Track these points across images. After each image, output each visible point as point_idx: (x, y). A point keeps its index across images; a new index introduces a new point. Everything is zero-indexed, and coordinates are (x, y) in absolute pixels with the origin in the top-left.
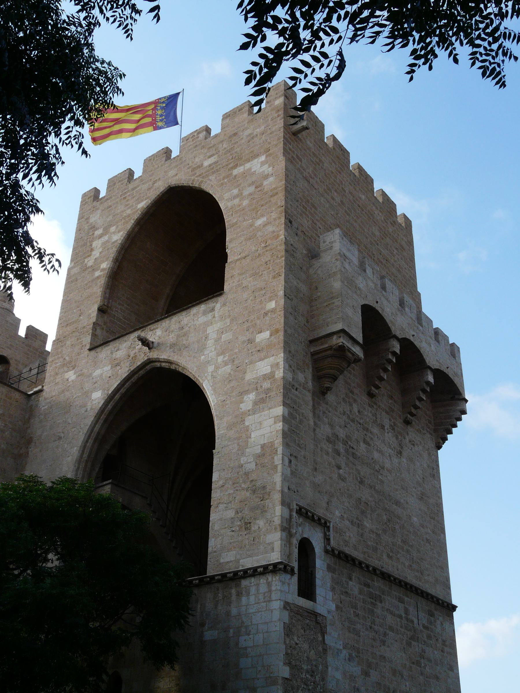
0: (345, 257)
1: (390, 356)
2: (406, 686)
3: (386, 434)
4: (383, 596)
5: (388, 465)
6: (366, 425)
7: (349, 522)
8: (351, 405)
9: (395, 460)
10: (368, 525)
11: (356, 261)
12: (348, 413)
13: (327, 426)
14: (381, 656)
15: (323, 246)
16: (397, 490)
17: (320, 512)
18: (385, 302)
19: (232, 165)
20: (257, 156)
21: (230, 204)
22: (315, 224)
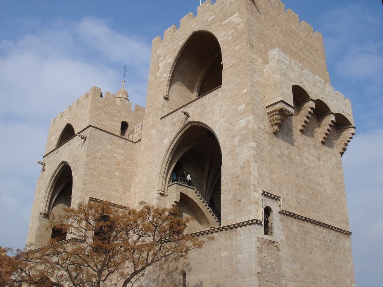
2: (323, 272)
5: (312, 165)
9: (317, 163)
10: (302, 197)
14: (310, 259)
15: (270, 57)
19: (222, 19)
20: (233, 13)
21: (222, 40)
22: (267, 45)
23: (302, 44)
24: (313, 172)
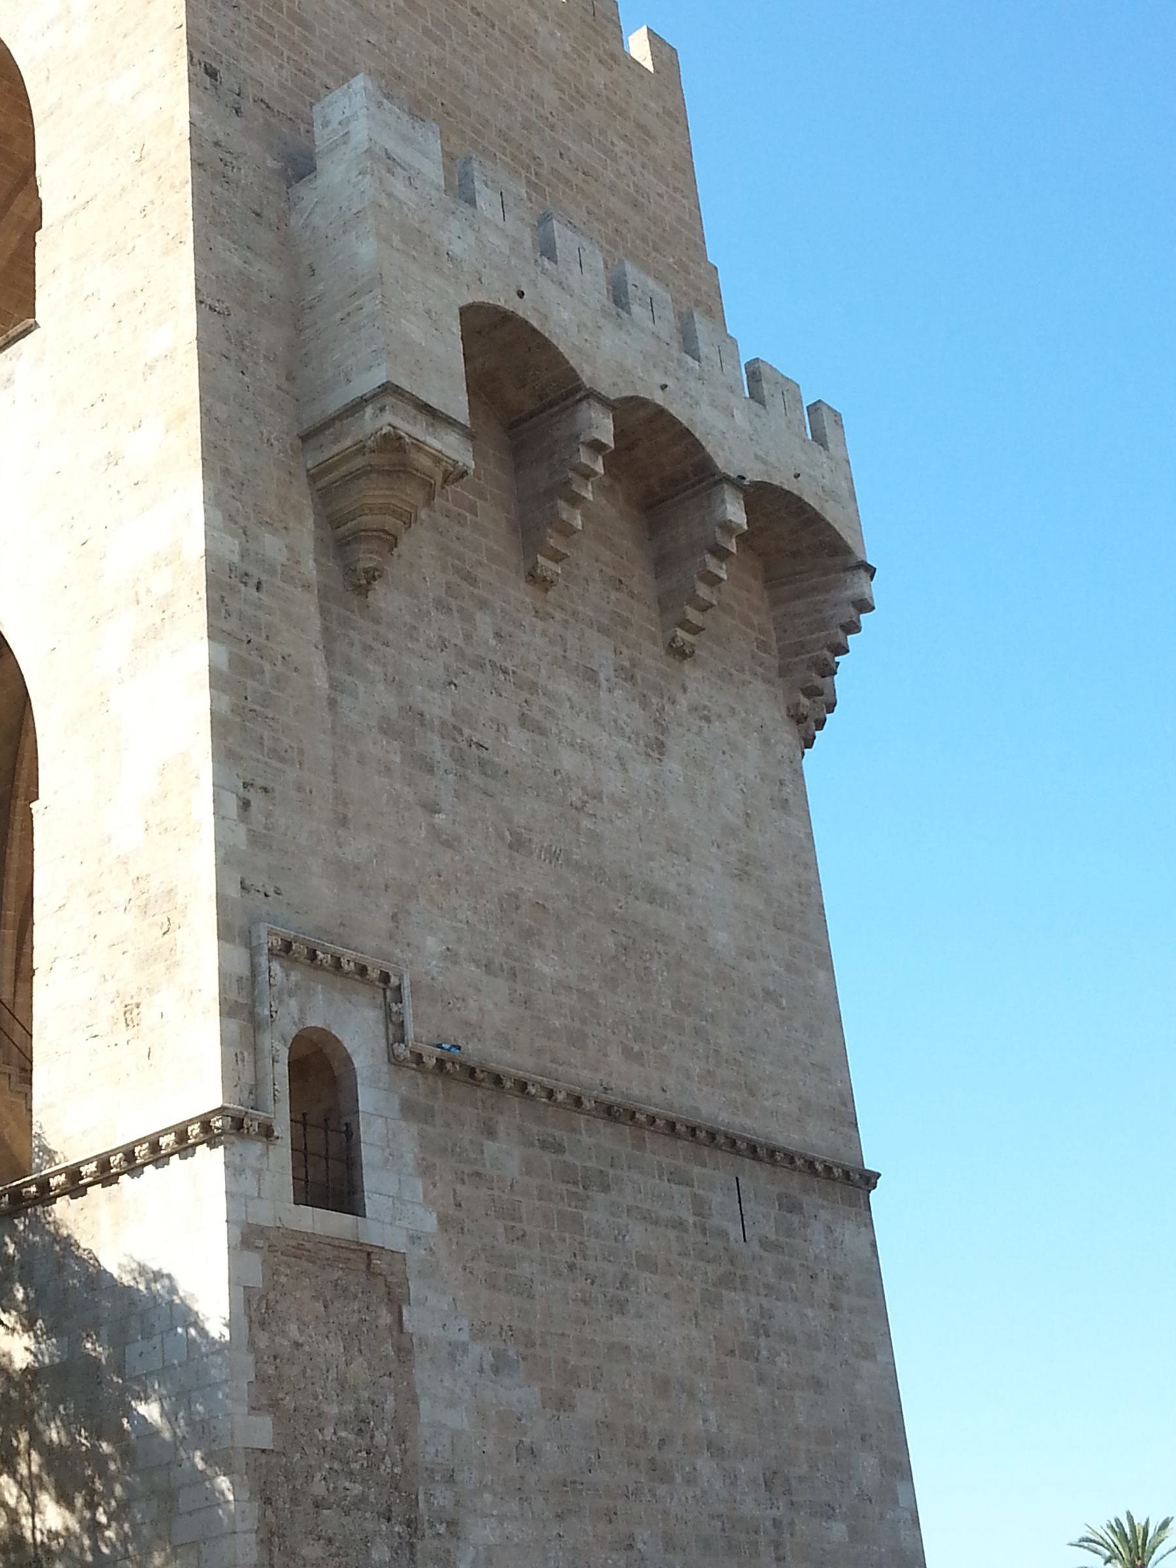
1: (584, 457)
3: (603, 694)
4: (611, 1172)
6: (529, 675)
7: (478, 967)
8: (467, 617)
9: (642, 771)
10: (547, 970)
11: (433, 170)
12: (459, 641)
13: (381, 687)
14: (611, 1347)
16: (651, 857)
17: (368, 943)
18: (552, 292)
22: (312, 76)
23: (551, 94)
24: (618, 822)
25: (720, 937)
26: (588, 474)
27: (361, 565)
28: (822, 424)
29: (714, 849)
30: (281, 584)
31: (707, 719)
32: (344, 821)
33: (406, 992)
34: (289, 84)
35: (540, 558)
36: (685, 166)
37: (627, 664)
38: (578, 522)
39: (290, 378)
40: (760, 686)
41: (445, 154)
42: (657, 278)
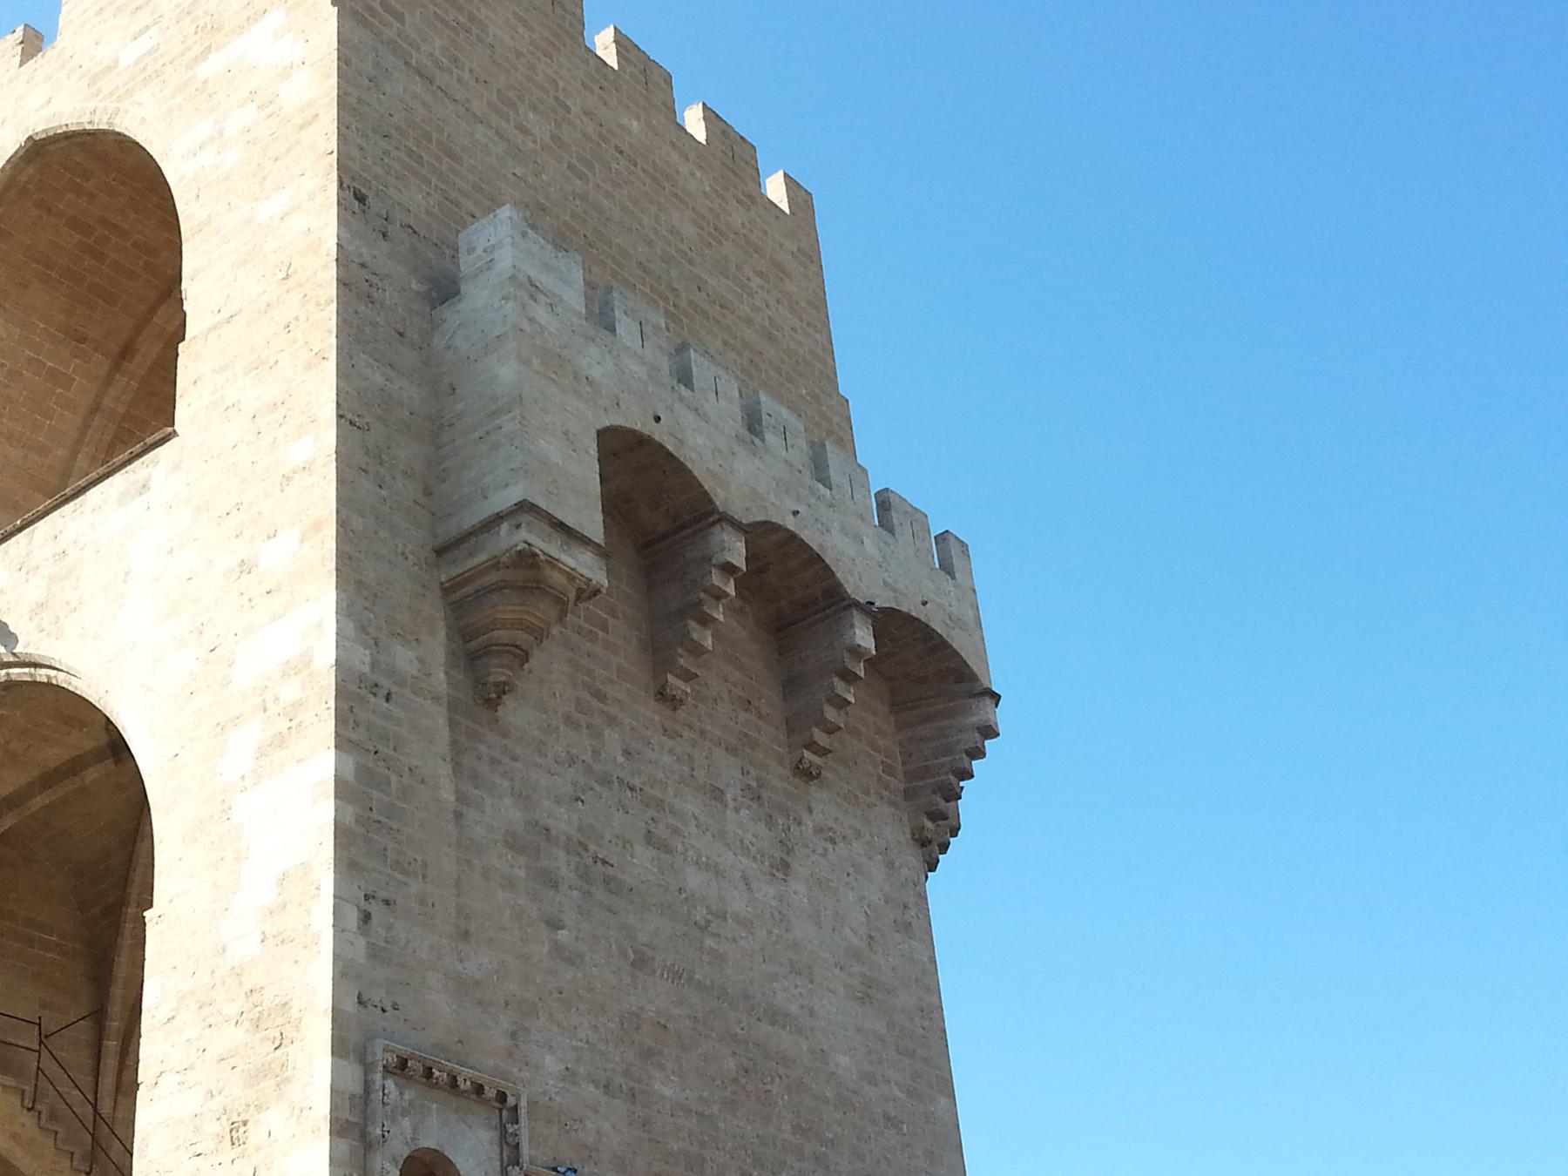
0: (534, 289)
1: (716, 579)
3: (730, 813)
5: (737, 903)
6: (656, 792)
8: (596, 734)
10: (667, 1092)
11: (574, 299)
12: (587, 757)
15: (466, 263)
16: (773, 978)
18: (689, 419)
24: (742, 943)
25: (843, 1062)
26: (719, 595)
27: (491, 679)
28: (949, 553)
29: (837, 971)
30: (412, 696)
31: (833, 841)
32: (465, 935)
33: (523, 1112)
34: (436, 210)
35: (670, 677)
36: (819, 303)
37: (754, 784)
38: (709, 643)
39: (428, 493)
40: (886, 809)
41: (587, 283)
42: (792, 407)
